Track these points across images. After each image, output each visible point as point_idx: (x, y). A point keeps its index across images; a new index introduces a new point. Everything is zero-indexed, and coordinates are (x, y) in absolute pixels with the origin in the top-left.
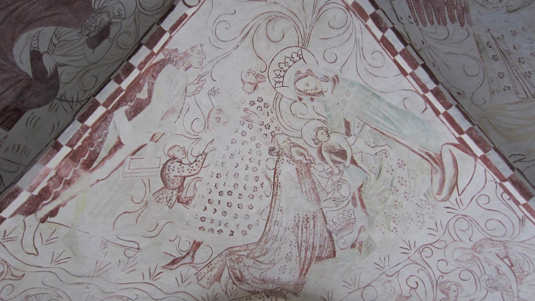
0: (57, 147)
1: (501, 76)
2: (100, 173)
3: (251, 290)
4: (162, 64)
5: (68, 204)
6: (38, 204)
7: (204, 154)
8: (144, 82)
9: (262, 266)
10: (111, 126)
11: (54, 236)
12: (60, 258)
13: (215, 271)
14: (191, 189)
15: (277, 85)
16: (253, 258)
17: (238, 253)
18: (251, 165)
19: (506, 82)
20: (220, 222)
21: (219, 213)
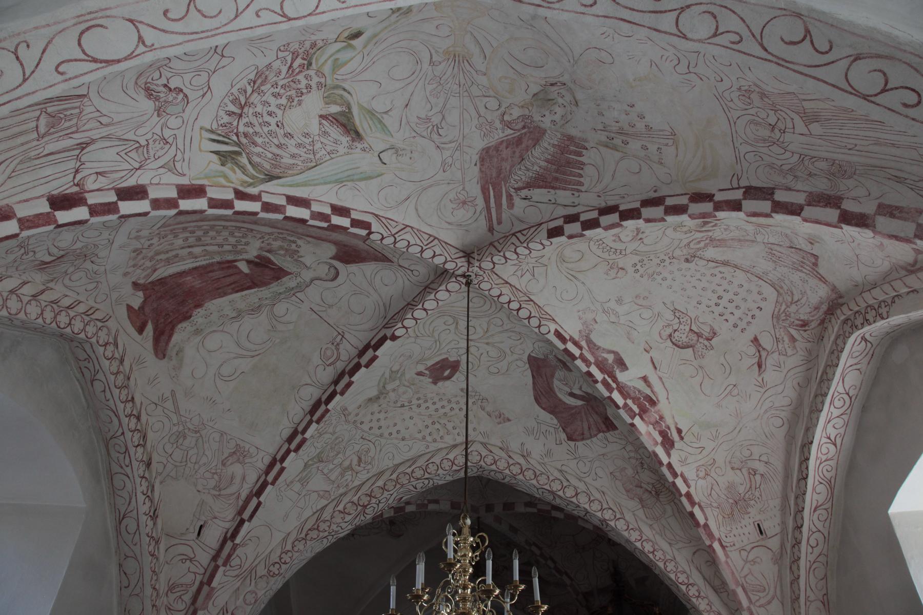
0: (633, 425)
1: (644, 148)
2: (661, 395)
3: (819, 321)
4: (589, 342)
5: (677, 421)
6: (669, 439)
7: (675, 311)
8: (601, 356)
9: (803, 301)
10: (629, 384)
11: (696, 435)
12: (714, 435)
13: (786, 339)
14: (703, 326)
15: (623, 253)
16: (791, 303)
17: (781, 311)
18: (698, 276)
19: (653, 148)
20: (744, 313)
21: (735, 311)
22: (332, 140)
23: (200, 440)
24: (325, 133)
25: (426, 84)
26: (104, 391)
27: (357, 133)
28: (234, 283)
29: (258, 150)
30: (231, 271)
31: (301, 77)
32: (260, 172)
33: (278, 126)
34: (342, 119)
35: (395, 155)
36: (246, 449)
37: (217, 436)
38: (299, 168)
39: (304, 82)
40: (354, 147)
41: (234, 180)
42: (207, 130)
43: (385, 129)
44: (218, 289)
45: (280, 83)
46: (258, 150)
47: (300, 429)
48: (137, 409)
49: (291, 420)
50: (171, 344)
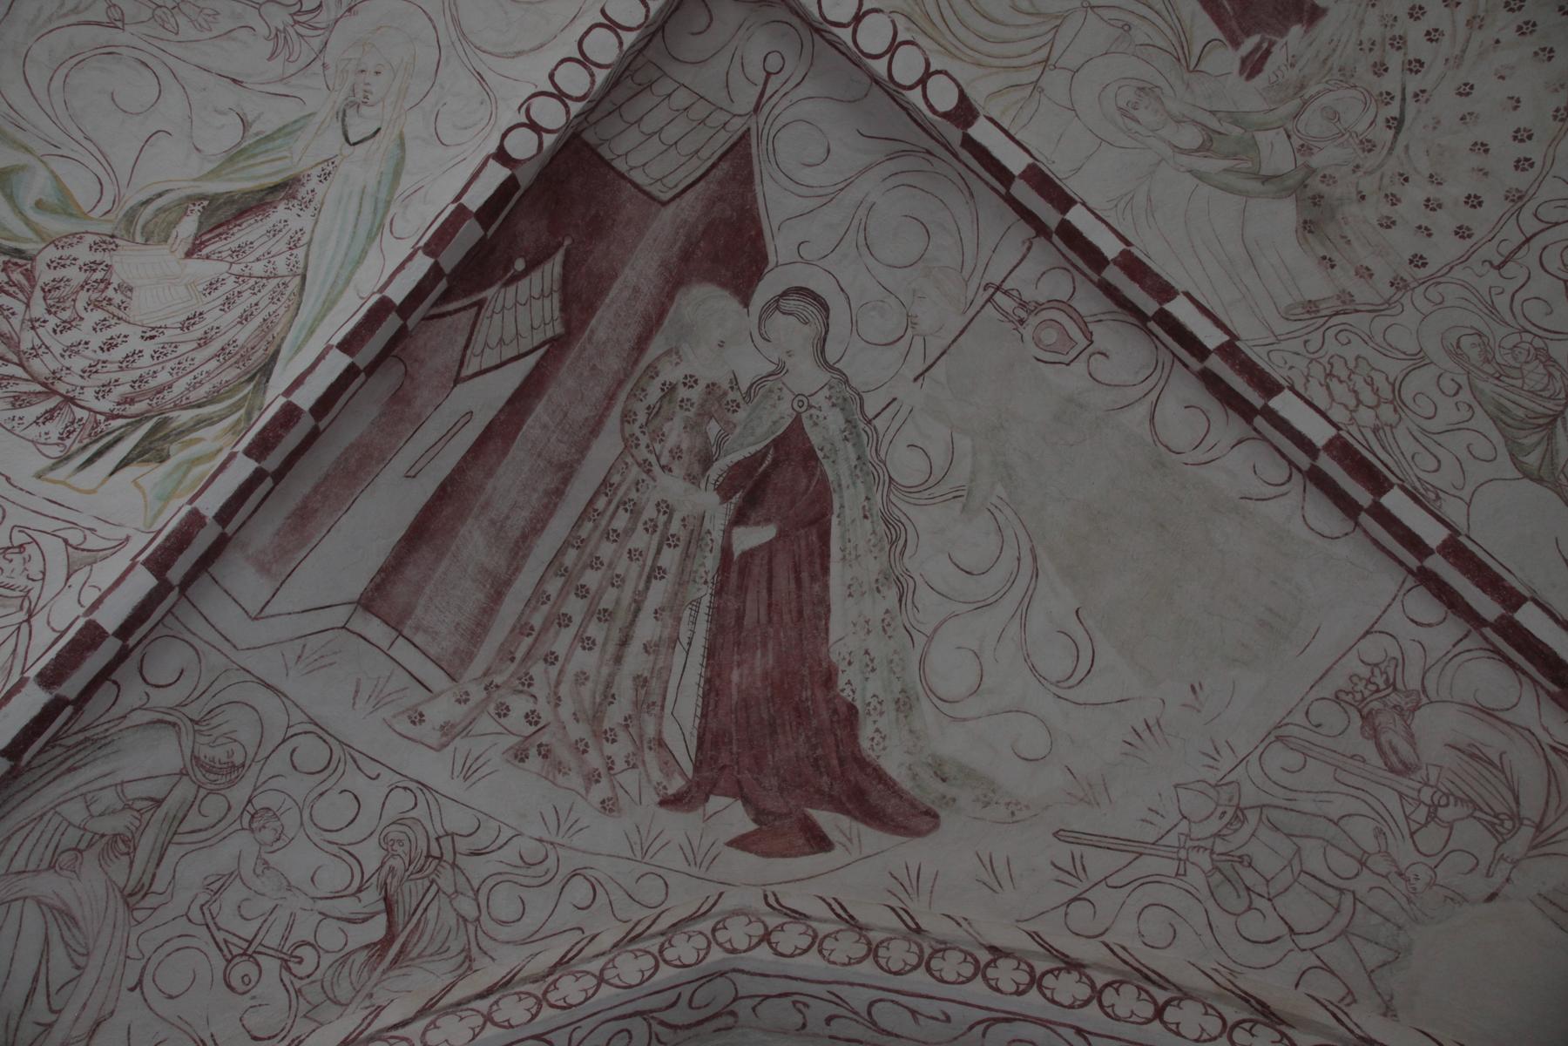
22: (265, 238)
23: (1276, 815)
24: (238, 252)
25: (178, 38)
26: (914, 1013)
27: (275, 189)
28: (797, 571)
29: (180, 387)
30: (758, 569)
31: (45, 276)
32: (232, 392)
33: (152, 337)
34: (221, 215)
35: (364, 109)
36: (1365, 672)
37: (1280, 757)
38: (281, 312)
39: (75, 275)
40: (310, 196)
41: (217, 445)
42: (52, 468)
43: (286, 130)
44: (800, 613)
45: (38, 309)
46: (180, 387)
47: (1304, 461)
48: (1035, 953)
49: (1272, 491)
50: (906, 784)
